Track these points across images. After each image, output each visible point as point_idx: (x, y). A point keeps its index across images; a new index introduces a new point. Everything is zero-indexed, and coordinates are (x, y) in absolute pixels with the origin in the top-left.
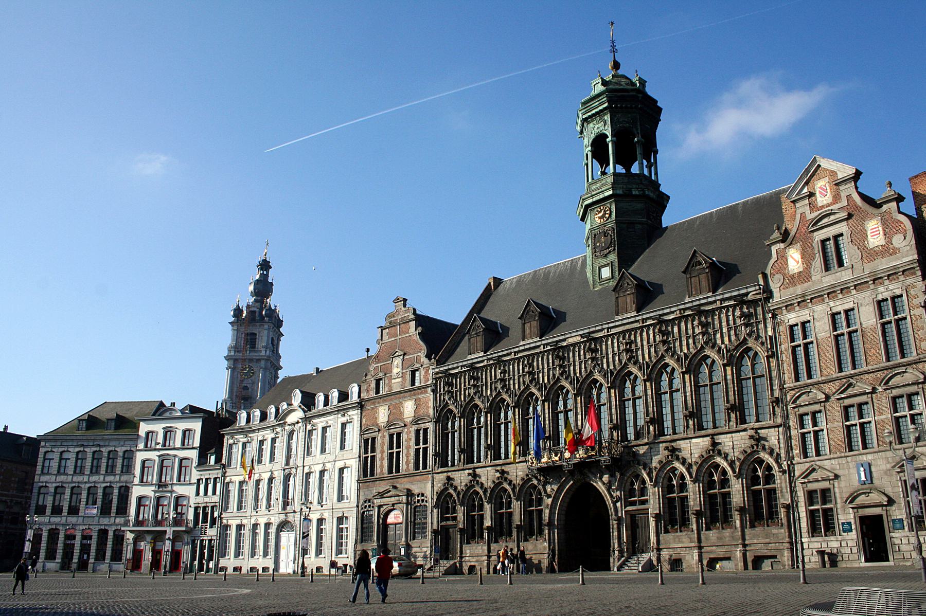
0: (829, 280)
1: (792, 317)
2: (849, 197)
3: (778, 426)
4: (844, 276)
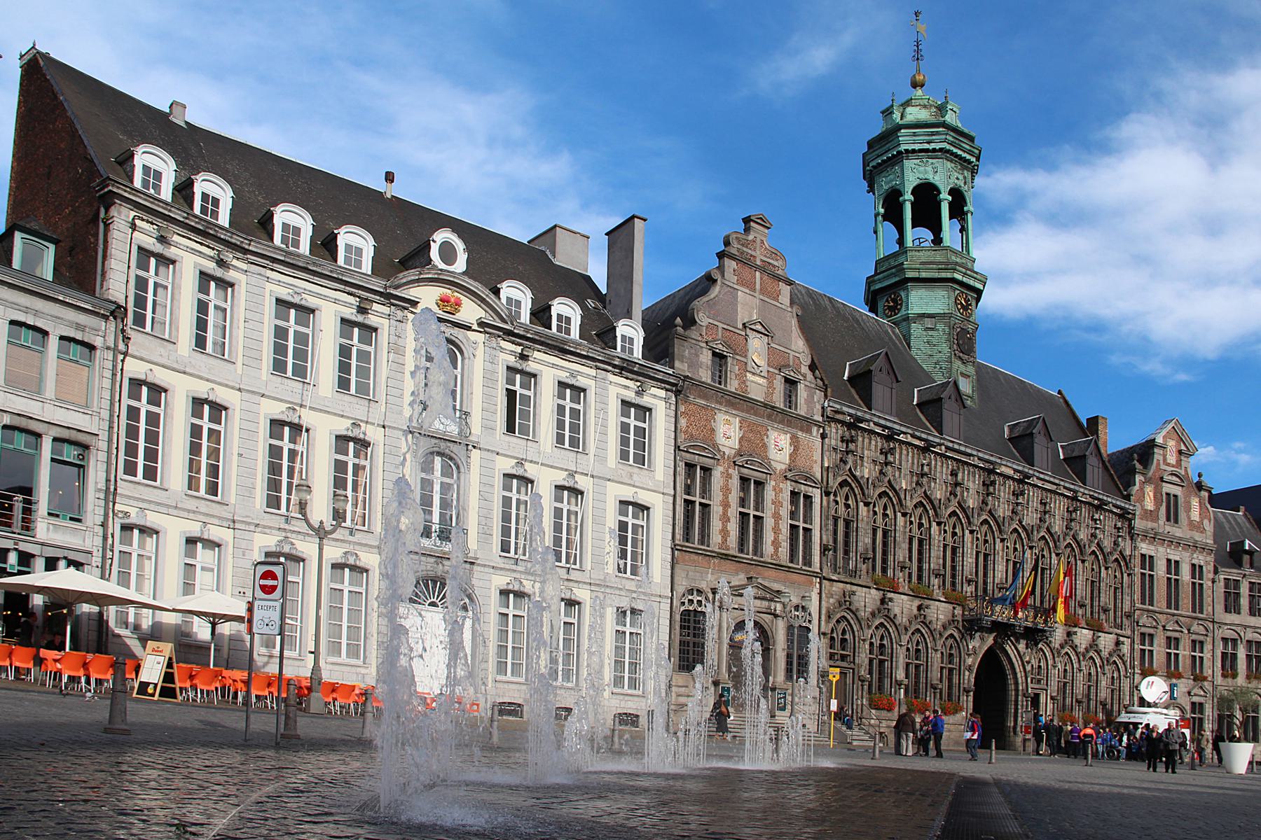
4: (1177, 532)
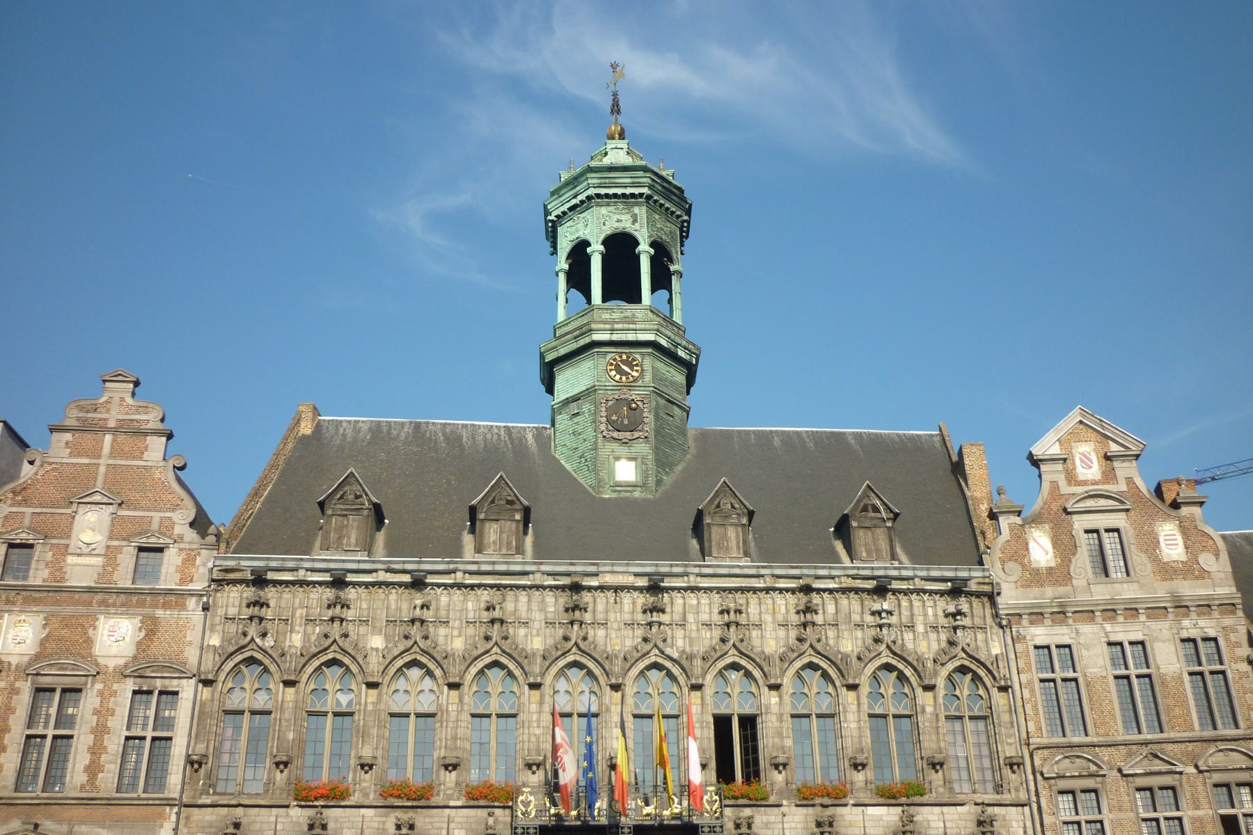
0: (1101, 592)
1: (1040, 634)
2: (1129, 481)
3: (1023, 805)
4: (1129, 592)
